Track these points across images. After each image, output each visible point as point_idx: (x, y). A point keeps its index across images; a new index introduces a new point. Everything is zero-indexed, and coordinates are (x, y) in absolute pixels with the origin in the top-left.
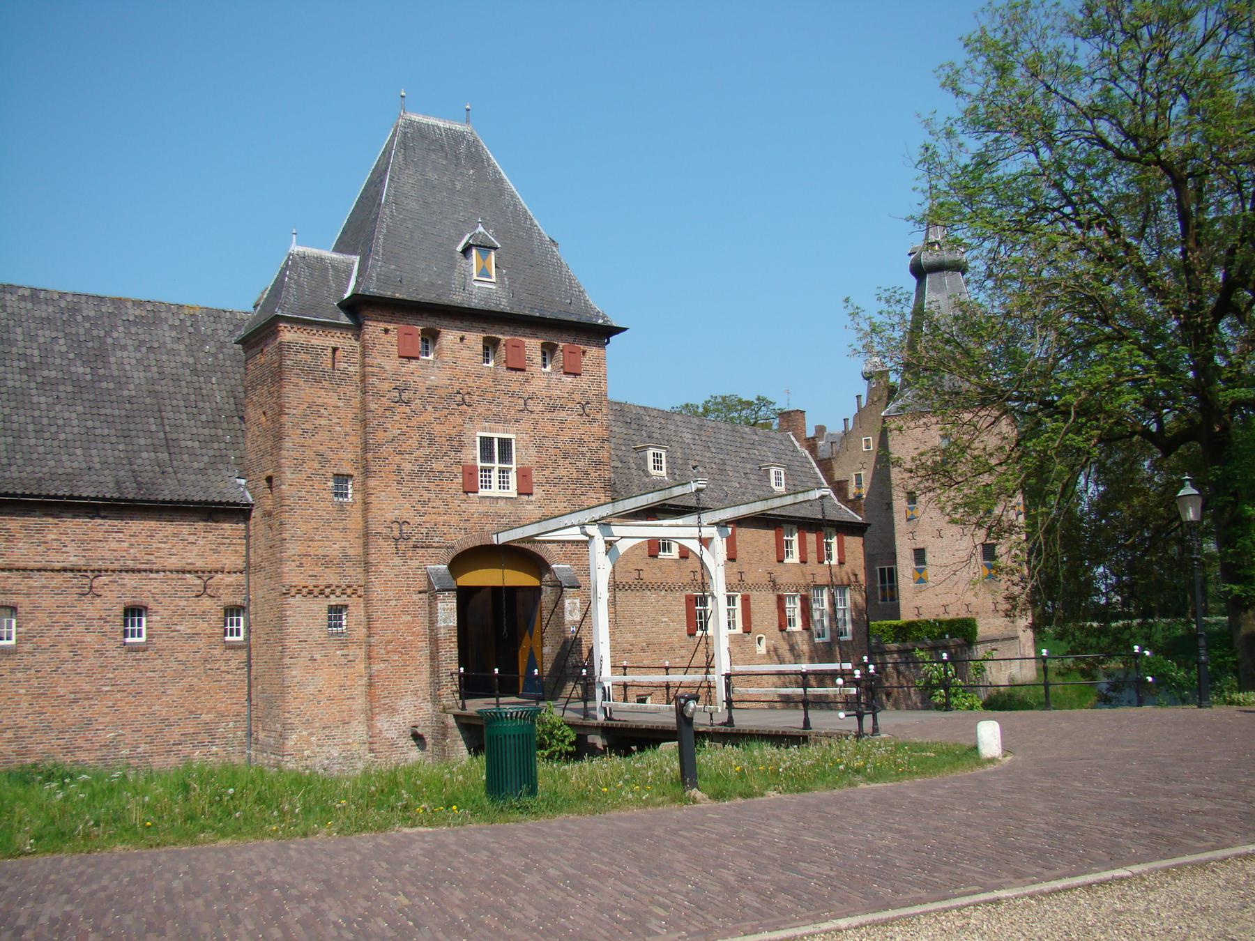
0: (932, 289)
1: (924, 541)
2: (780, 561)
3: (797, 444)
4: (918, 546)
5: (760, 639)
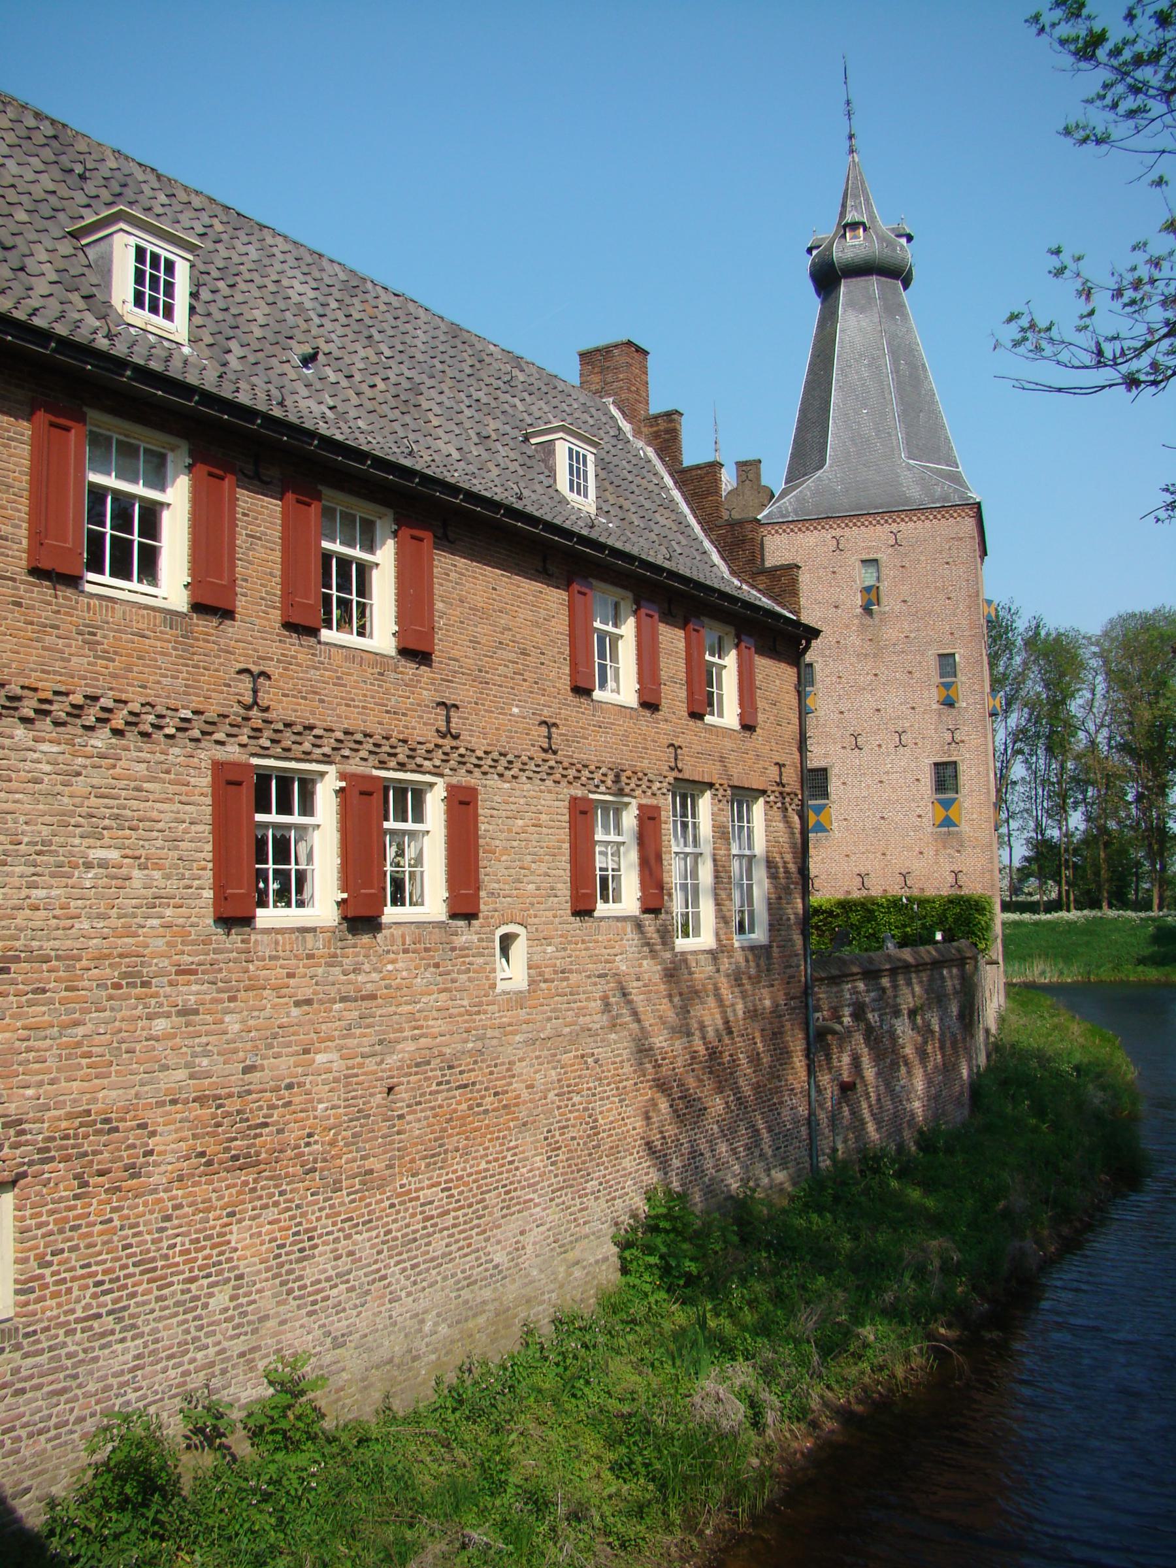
0: (851, 304)
1: (826, 755)
2: (582, 691)
3: (626, 427)
5: (507, 941)
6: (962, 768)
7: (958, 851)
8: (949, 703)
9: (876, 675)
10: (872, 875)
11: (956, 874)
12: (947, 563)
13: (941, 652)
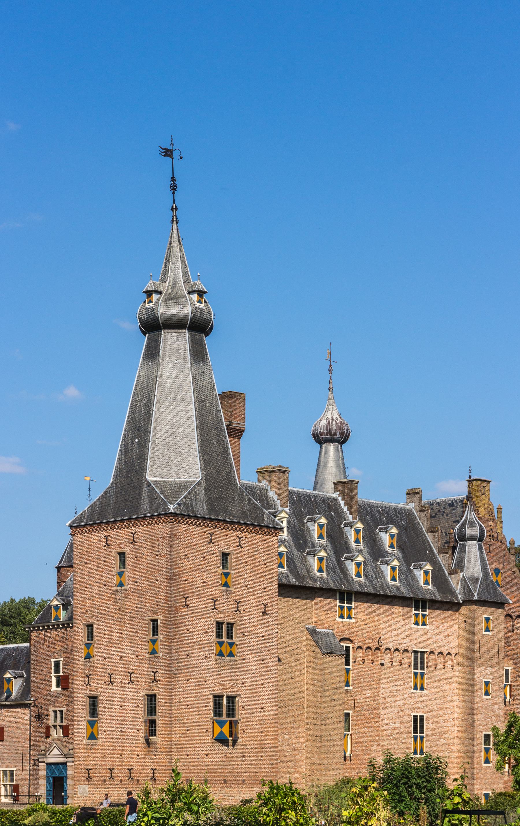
4: (93, 694)
6: (158, 698)
7: (155, 755)
8: (154, 652)
9: (121, 633)
10: (116, 769)
11: (153, 770)
12: (157, 555)
13: (152, 618)
